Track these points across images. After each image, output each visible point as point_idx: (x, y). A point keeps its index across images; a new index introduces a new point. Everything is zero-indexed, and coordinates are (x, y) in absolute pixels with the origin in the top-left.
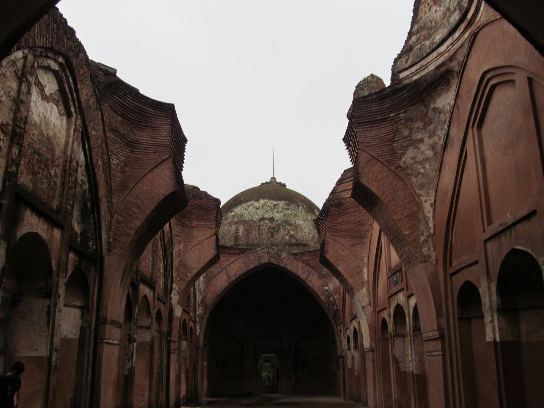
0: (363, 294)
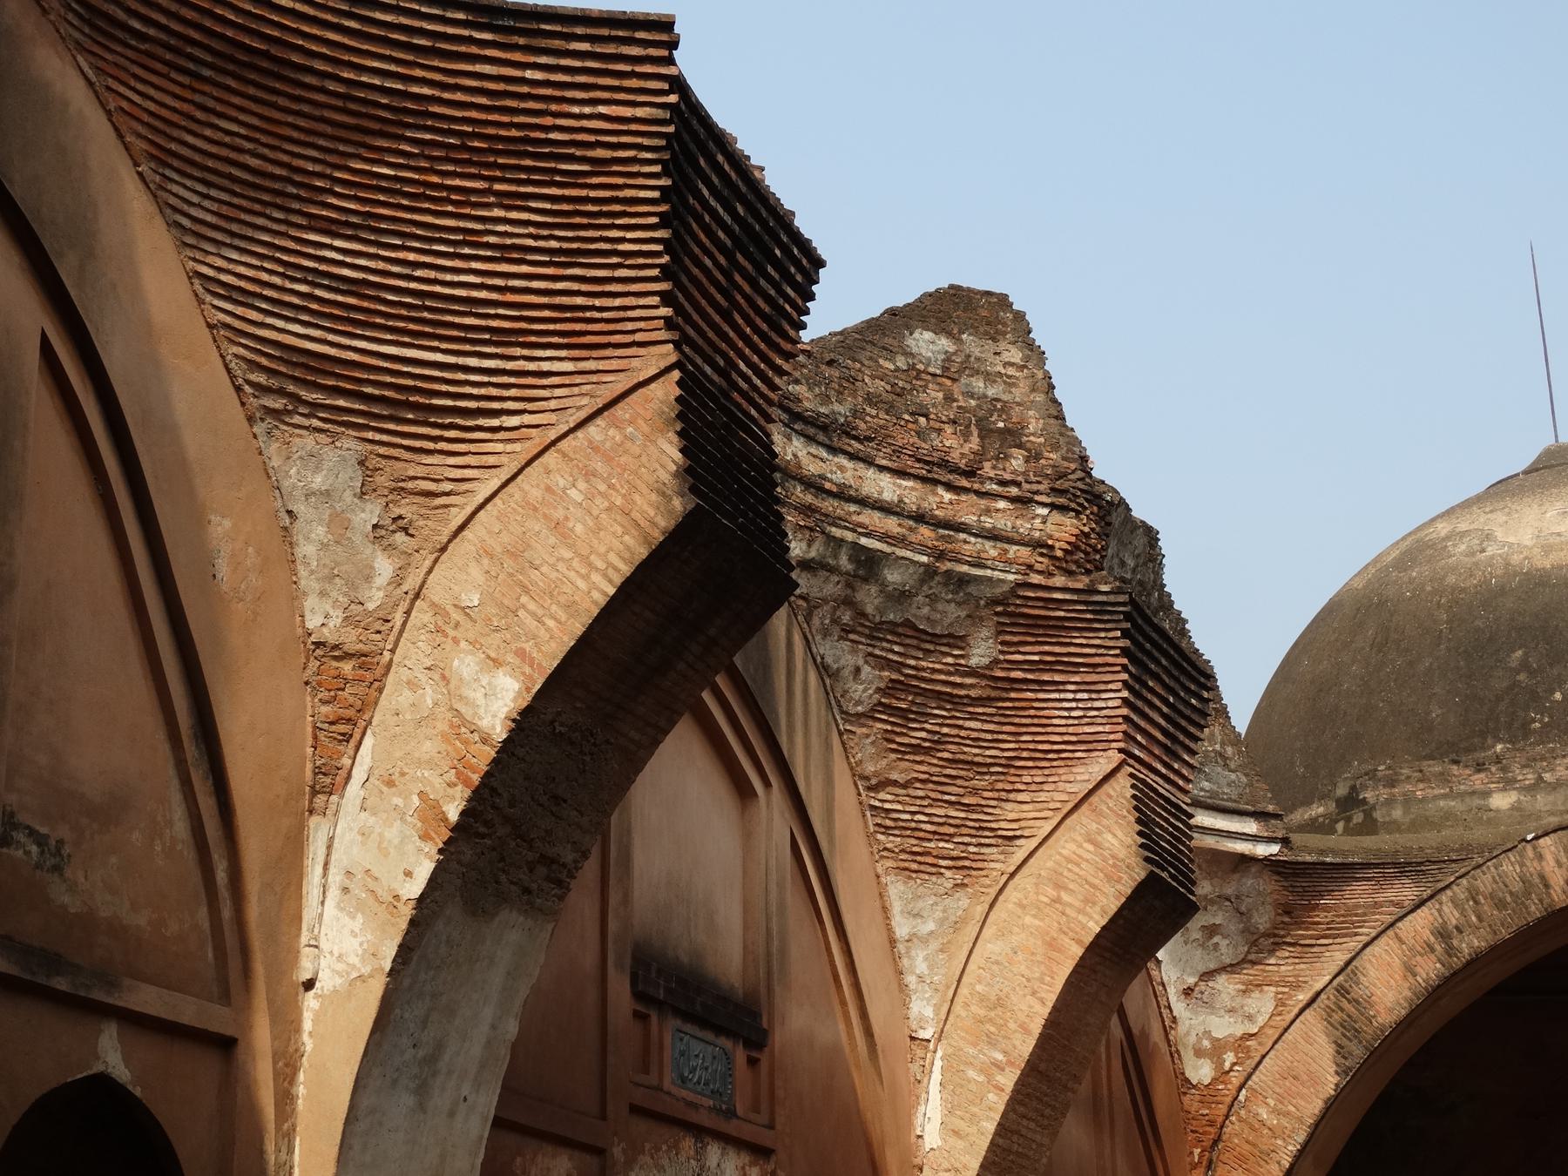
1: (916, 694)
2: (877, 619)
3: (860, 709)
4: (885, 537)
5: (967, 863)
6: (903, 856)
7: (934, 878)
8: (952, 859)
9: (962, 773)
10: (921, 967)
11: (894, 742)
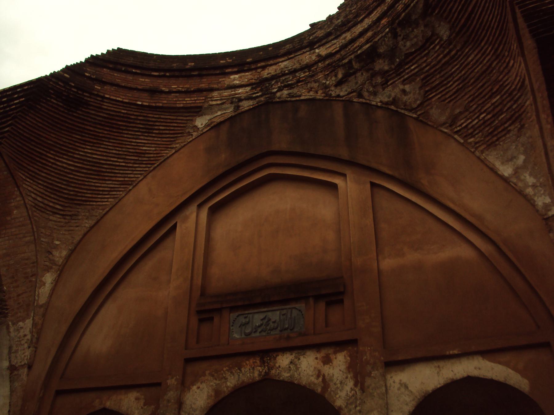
0: (21, 334)
1: (440, 73)
2: (393, 67)
3: (418, 102)
4: (367, 42)
5: (517, 115)
6: (487, 139)
7: (508, 136)
8: (510, 119)
9: (484, 81)
10: (530, 180)
11: (446, 99)
